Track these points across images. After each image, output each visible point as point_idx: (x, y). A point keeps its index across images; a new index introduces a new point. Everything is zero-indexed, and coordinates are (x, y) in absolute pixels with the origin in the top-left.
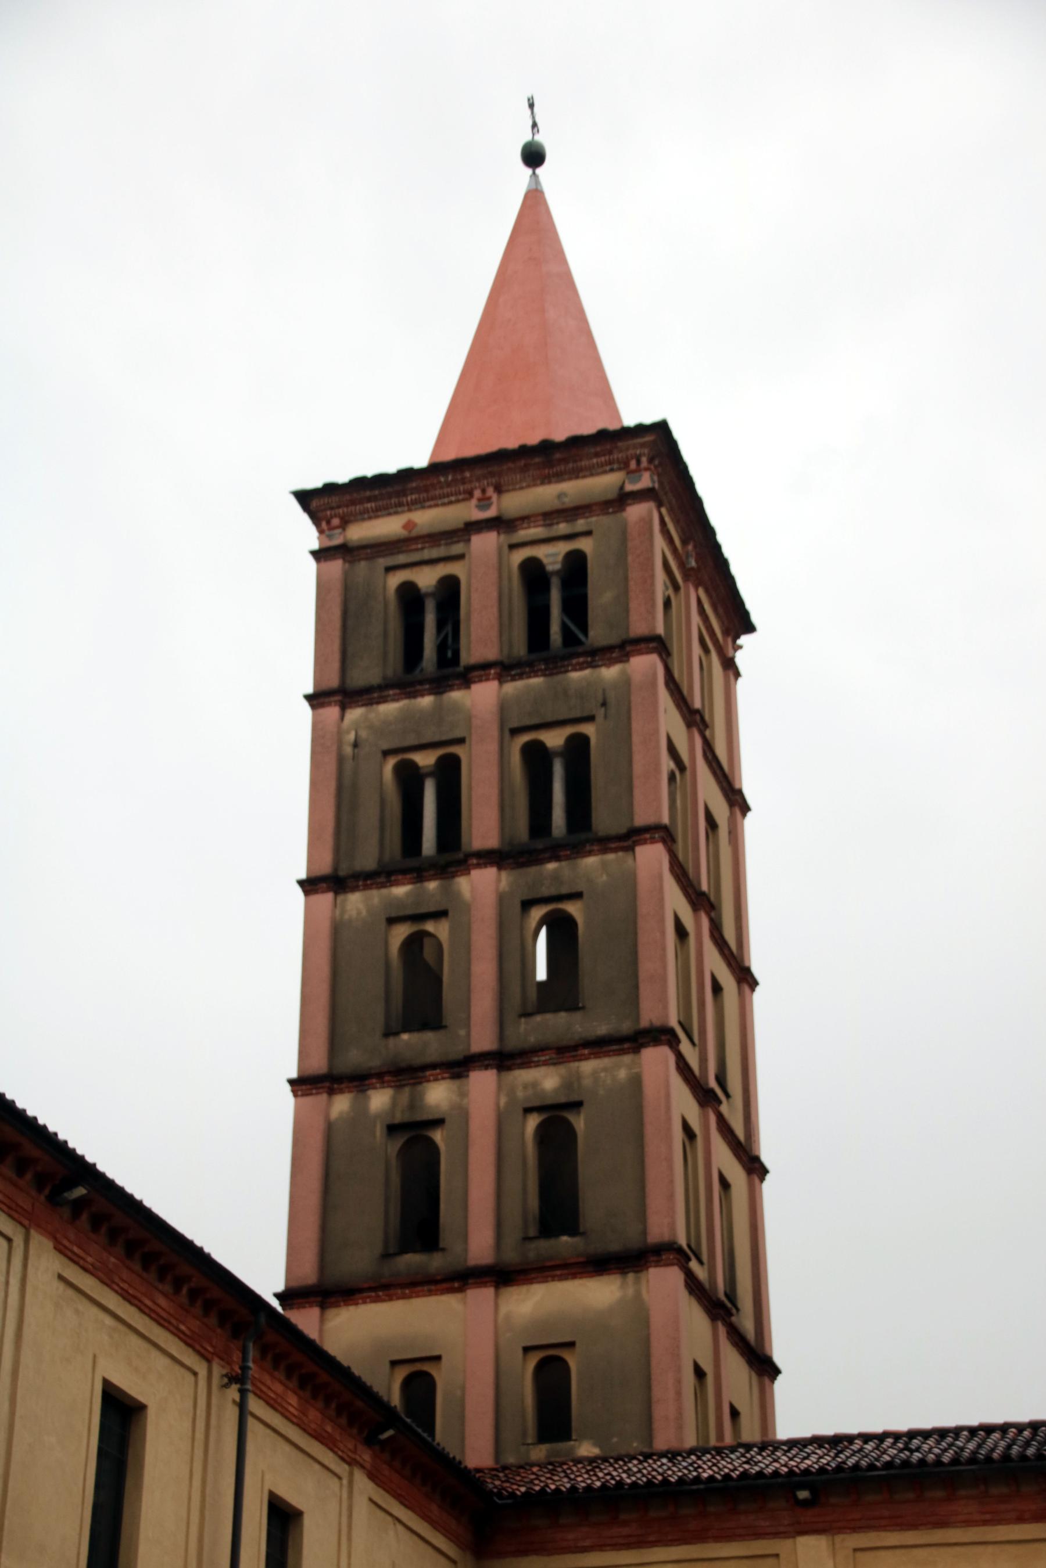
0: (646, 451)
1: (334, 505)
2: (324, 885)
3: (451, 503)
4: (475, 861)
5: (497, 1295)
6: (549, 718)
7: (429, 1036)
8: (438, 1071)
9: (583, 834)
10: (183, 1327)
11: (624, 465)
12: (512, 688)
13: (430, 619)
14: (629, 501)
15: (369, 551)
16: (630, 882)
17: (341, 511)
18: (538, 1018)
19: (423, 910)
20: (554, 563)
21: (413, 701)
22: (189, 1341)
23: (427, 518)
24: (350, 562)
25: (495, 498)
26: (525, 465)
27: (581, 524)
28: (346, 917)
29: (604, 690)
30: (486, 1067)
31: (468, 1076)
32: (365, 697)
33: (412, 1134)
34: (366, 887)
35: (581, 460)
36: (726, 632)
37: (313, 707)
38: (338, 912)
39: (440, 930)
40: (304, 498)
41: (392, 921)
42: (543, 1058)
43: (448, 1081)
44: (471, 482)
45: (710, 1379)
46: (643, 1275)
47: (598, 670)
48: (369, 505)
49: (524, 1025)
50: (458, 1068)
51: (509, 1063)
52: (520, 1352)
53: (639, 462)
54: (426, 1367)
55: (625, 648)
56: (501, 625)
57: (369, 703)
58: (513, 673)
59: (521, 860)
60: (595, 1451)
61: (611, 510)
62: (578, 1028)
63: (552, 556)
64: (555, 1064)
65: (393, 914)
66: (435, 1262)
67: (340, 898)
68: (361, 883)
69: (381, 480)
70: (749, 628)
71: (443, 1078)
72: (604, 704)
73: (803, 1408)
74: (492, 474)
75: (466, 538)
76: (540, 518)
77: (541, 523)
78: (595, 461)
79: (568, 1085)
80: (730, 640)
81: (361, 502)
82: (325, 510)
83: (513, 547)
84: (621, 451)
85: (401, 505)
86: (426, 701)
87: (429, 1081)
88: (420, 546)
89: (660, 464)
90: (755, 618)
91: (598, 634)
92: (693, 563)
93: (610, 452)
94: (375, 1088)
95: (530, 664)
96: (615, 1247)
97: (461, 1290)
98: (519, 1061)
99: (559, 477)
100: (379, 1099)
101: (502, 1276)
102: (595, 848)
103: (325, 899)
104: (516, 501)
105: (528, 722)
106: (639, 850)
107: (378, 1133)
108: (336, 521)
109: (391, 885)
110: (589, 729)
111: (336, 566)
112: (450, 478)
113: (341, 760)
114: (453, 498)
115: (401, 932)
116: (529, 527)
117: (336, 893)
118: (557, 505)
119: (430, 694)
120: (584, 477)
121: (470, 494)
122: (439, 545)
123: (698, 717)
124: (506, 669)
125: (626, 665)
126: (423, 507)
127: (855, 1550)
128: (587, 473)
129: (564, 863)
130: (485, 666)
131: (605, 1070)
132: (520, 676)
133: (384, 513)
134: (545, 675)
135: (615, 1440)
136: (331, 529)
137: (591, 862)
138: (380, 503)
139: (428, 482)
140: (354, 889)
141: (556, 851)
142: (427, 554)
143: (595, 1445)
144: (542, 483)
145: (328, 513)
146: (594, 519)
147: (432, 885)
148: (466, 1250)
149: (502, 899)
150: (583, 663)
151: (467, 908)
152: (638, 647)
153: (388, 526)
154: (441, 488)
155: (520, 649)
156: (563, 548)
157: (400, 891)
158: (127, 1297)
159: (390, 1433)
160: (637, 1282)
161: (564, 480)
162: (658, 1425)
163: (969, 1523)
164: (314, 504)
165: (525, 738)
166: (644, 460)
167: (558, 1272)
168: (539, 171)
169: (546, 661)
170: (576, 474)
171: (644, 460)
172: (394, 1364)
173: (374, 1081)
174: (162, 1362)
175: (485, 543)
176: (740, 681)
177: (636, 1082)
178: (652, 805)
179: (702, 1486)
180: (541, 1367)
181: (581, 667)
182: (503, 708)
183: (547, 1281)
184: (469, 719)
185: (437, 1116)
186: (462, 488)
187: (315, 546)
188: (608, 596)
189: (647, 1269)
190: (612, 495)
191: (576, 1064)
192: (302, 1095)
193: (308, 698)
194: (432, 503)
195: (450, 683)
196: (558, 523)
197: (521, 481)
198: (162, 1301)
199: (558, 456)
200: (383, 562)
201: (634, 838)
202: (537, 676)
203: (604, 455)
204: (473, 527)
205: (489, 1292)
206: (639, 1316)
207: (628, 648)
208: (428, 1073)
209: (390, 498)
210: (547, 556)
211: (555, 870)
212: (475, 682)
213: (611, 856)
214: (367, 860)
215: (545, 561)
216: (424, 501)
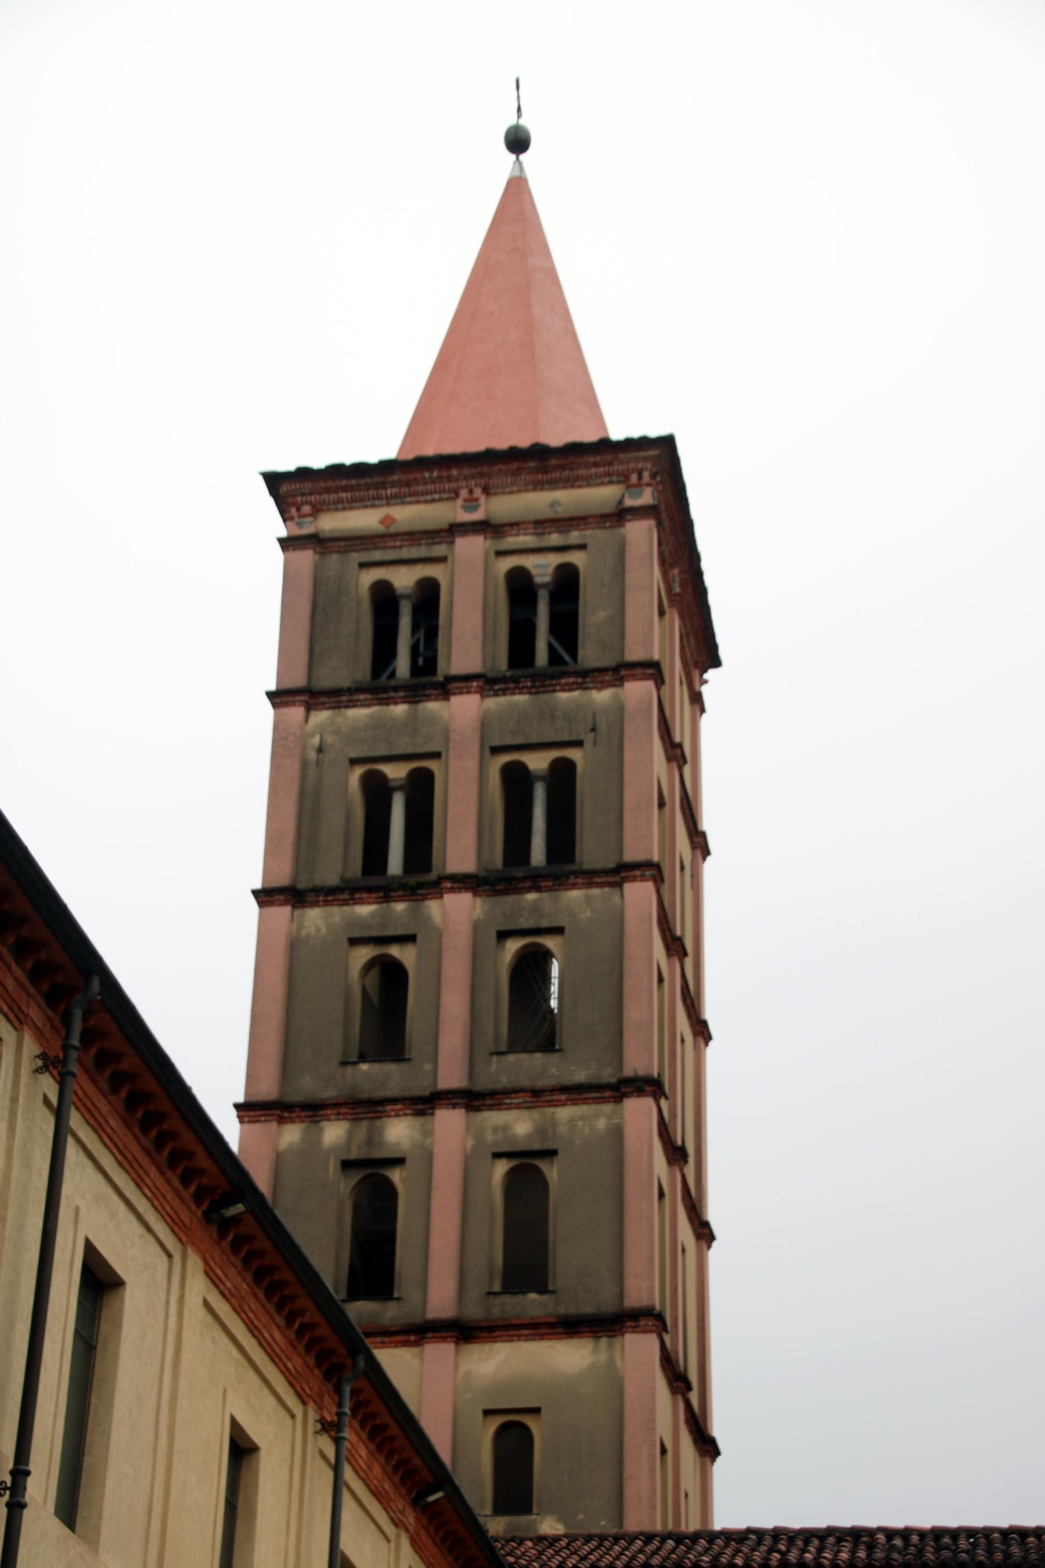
0: (649, 466)
1: (307, 491)
2: (282, 897)
3: (433, 501)
4: (449, 885)
5: (457, 1352)
6: (534, 739)
7: (391, 1068)
8: (400, 1106)
9: (564, 865)
10: (290, 1365)
12: (493, 703)
13: (405, 622)
14: (629, 517)
15: (342, 544)
17: (313, 498)
18: (512, 1058)
19: (389, 933)
20: (542, 575)
21: (385, 708)
23: (407, 515)
24: (322, 554)
25: (483, 499)
26: (518, 469)
27: (574, 537)
28: (304, 933)
29: (594, 715)
30: (454, 1106)
31: (433, 1114)
32: (334, 699)
33: (369, 1172)
34: (327, 903)
35: (578, 469)
37: (275, 705)
38: (294, 927)
39: (405, 955)
40: (274, 481)
41: (354, 942)
42: (516, 1101)
43: (410, 1118)
44: (457, 480)
45: (670, 1455)
46: (617, 1341)
47: (588, 692)
48: (344, 495)
49: (495, 1062)
50: (425, 1104)
51: (476, 1103)
52: (480, 1415)
55: (619, 672)
56: (485, 636)
58: (496, 687)
59: (499, 887)
61: (608, 524)
62: (554, 1071)
63: (542, 568)
64: (528, 1108)
65: (357, 935)
67: (298, 912)
68: (321, 898)
70: (716, 663)
71: (405, 1115)
72: (593, 729)
74: (482, 475)
75: (449, 539)
76: (531, 526)
77: (532, 531)
78: (593, 471)
79: (541, 1131)
81: (336, 490)
82: (296, 495)
83: (500, 554)
84: (621, 463)
85: (379, 498)
86: (400, 710)
87: (389, 1116)
88: (398, 543)
89: (661, 482)
90: (723, 653)
91: (590, 654)
92: (677, 589)
93: (611, 464)
94: (329, 1120)
95: (516, 680)
96: (588, 1309)
98: (488, 1102)
99: (553, 484)
100: (334, 1132)
101: (464, 1331)
102: (579, 881)
103: (282, 913)
104: (504, 505)
105: (509, 741)
106: (628, 887)
107: (331, 1169)
108: (306, 509)
109: (355, 904)
110: (574, 754)
111: (306, 557)
112: (435, 474)
113: (304, 764)
114: (437, 496)
115: (364, 954)
116: (517, 535)
118: (550, 514)
119: (404, 702)
120: (580, 487)
121: (457, 494)
122: (420, 545)
123: (678, 751)
124: (488, 683)
125: (619, 690)
126: (403, 503)
128: (584, 483)
129: (545, 895)
130: (468, 678)
131: (582, 1118)
132: (504, 692)
133: (359, 504)
134: (530, 693)
135: (581, 1516)
136: (301, 516)
137: (575, 895)
138: (357, 494)
139: (411, 477)
140: (315, 904)
141: (536, 881)
142: (405, 553)
143: (559, 1520)
144: (535, 489)
145: (299, 499)
146: (589, 532)
147: (400, 907)
148: (425, 1302)
149: (477, 928)
150: (573, 683)
151: (439, 935)
152: (634, 672)
153: (363, 520)
154: (425, 484)
155: (502, 664)
156: (554, 560)
157: (364, 910)
158: (253, 1329)
159: (439, 1495)
160: (611, 1347)
161: (557, 488)
162: (629, 1503)
164: (284, 488)
166: (646, 475)
167: (525, 1332)
168: (523, 157)
169: (533, 677)
170: (571, 483)
171: (646, 475)
173: (329, 1112)
174: (270, 1401)
175: (471, 549)
176: (704, 716)
177: (617, 1134)
178: (642, 841)
180: (502, 1431)
181: (571, 688)
182: (485, 724)
183: (512, 1341)
184: (446, 733)
186: (447, 486)
187: (283, 533)
188: (602, 615)
189: (623, 1334)
190: (609, 509)
191: (552, 1110)
192: (250, 1122)
193: (270, 695)
194: (413, 499)
195: (427, 692)
196: (550, 533)
197: (512, 485)
198: (278, 1336)
199: (554, 462)
200: (356, 557)
201: (624, 874)
202: (521, 693)
203: (604, 465)
204: (455, 530)
205: (449, 1348)
206: (614, 1386)
207: (623, 673)
208: (388, 1108)
209: (368, 489)
210: (536, 566)
211: (535, 901)
212: (454, 694)
213: (596, 892)
214: (329, 876)
215: (534, 572)
216: (405, 496)
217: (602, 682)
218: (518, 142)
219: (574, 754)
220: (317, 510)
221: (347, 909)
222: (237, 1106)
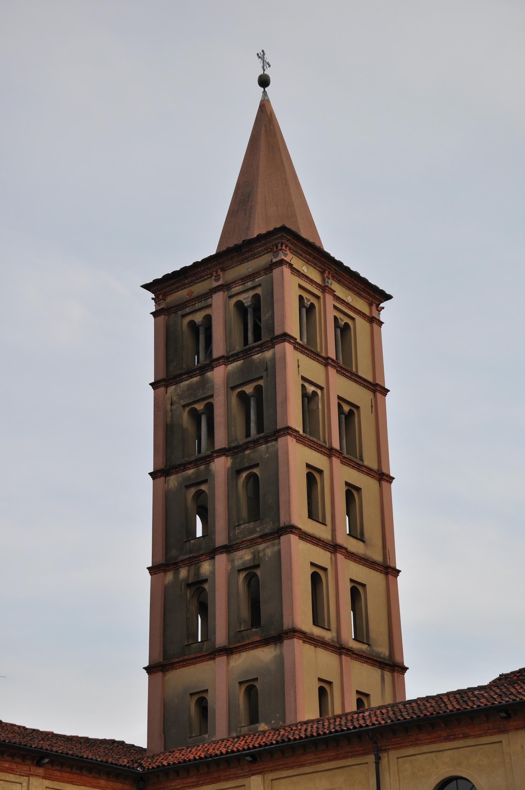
3: (205, 279)
5: (228, 659)
16: (275, 456)
25: (221, 273)
28: (170, 487)
30: (222, 553)
36: (370, 305)
37: (154, 389)
38: (166, 485)
41: (188, 487)
47: (264, 353)
50: (212, 553)
53: (277, 248)
54: (204, 695)
57: (177, 383)
60: (266, 727)
63: (246, 298)
69: (175, 273)
72: (266, 370)
73: (417, 686)
80: (374, 307)
83: (231, 297)
94: (182, 567)
97: (214, 658)
99: (247, 260)
100: (183, 573)
101: (228, 651)
108: (161, 297)
110: (261, 382)
111: (162, 318)
115: (193, 490)
117: (166, 477)
123: (330, 361)
127: (272, 780)
130: (218, 359)
142: (198, 306)
147: (202, 467)
150: (258, 351)
156: (251, 293)
157: (191, 472)
160: (281, 647)
163: (311, 764)
165: (239, 390)
167: (250, 646)
168: (267, 89)
170: (254, 256)
172: (192, 695)
175: (218, 299)
177: (279, 552)
179: (274, 746)
185: (205, 578)
187: (153, 310)
191: (257, 546)
217: (268, 347)
218: (264, 82)
219: (261, 382)
220: (165, 295)
221: (184, 473)
222: (148, 568)
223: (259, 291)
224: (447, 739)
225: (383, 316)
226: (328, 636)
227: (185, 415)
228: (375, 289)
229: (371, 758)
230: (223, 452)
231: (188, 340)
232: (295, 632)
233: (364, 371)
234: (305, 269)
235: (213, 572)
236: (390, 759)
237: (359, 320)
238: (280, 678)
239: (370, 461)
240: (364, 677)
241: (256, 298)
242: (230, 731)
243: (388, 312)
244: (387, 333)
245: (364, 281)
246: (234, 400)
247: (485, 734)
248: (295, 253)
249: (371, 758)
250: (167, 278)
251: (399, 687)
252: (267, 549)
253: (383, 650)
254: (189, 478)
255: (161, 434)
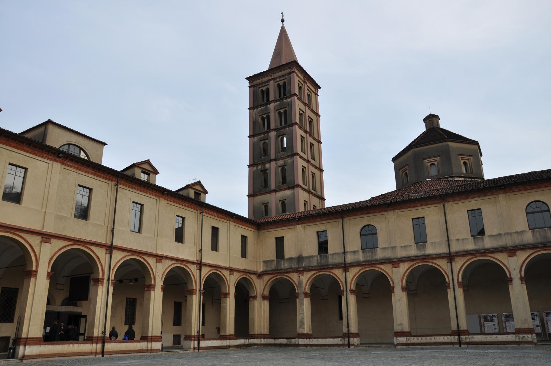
11: (290, 68)
16: (292, 131)
22: (193, 208)
40: (247, 79)
50: (270, 161)
63: (281, 83)
66: (268, 189)
69: (257, 75)
70: (320, 88)
79: (285, 162)
99: (281, 71)
100: (260, 167)
101: (276, 191)
110: (286, 109)
111: (252, 88)
115: (263, 142)
124: (275, 101)
155: (278, 98)
156: (283, 81)
170: (284, 70)
175: (272, 83)
182: (275, 106)
218: (283, 21)
219: (286, 109)
220: (253, 81)
223: (285, 80)
224: (367, 214)
225: (319, 93)
226: (306, 188)
227: (260, 118)
228: (317, 84)
229: (340, 220)
230: (273, 130)
231: (260, 96)
232: (298, 186)
233: (314, 109)
234: (299, 75)
235: (270, 167)
236: (347, 220)
237: (313, 94)
238: (294, 200)
239: (316, 137)
240: (315, 201)
241: (285, 83)
242: (276, 214)
243: (320, 92)
244: (320, 98)
245: (314, 82)
246: (277, 114)
247: (380, 212)
248: (297, 70)
249: (340, 220)
250: (254, 76)
251: (323, 204)
252: (289, 160)
253: (319, 194)
254: (261, 138)
255: (252, 124)
